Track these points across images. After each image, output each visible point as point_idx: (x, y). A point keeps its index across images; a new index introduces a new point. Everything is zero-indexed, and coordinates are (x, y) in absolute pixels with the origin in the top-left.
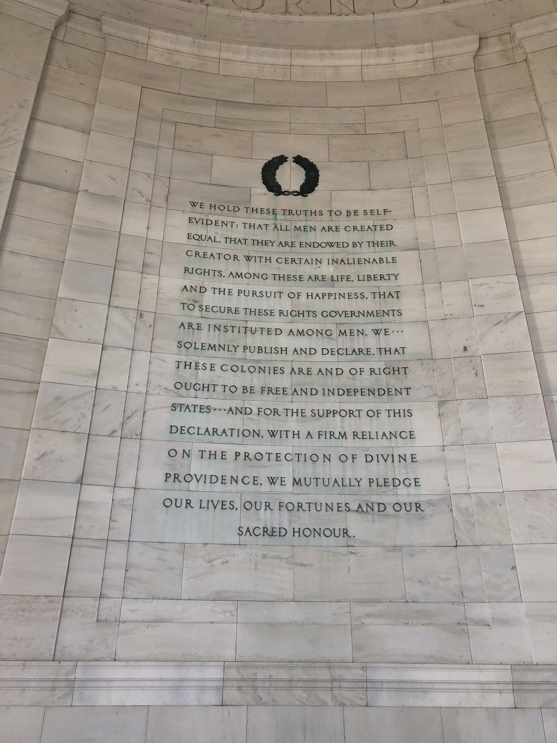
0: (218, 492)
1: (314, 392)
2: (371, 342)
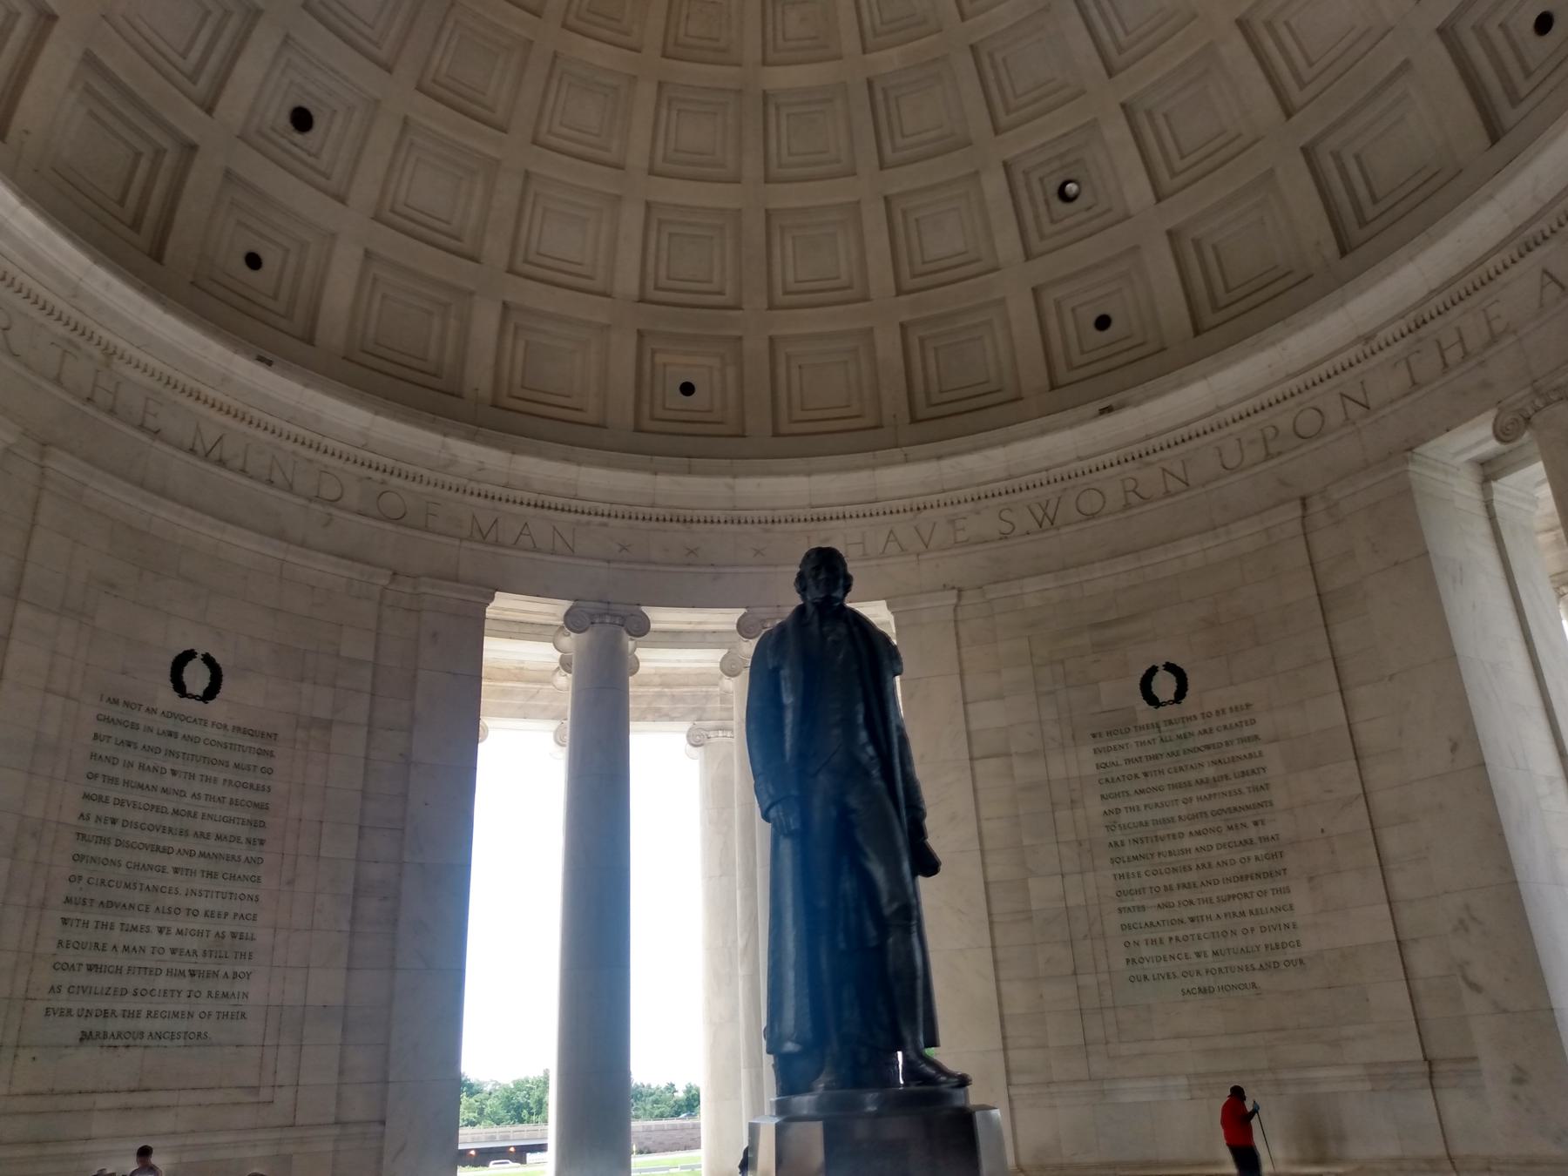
0: (1164, 967)
1: (1216, 882)
2: (1252, 833)
